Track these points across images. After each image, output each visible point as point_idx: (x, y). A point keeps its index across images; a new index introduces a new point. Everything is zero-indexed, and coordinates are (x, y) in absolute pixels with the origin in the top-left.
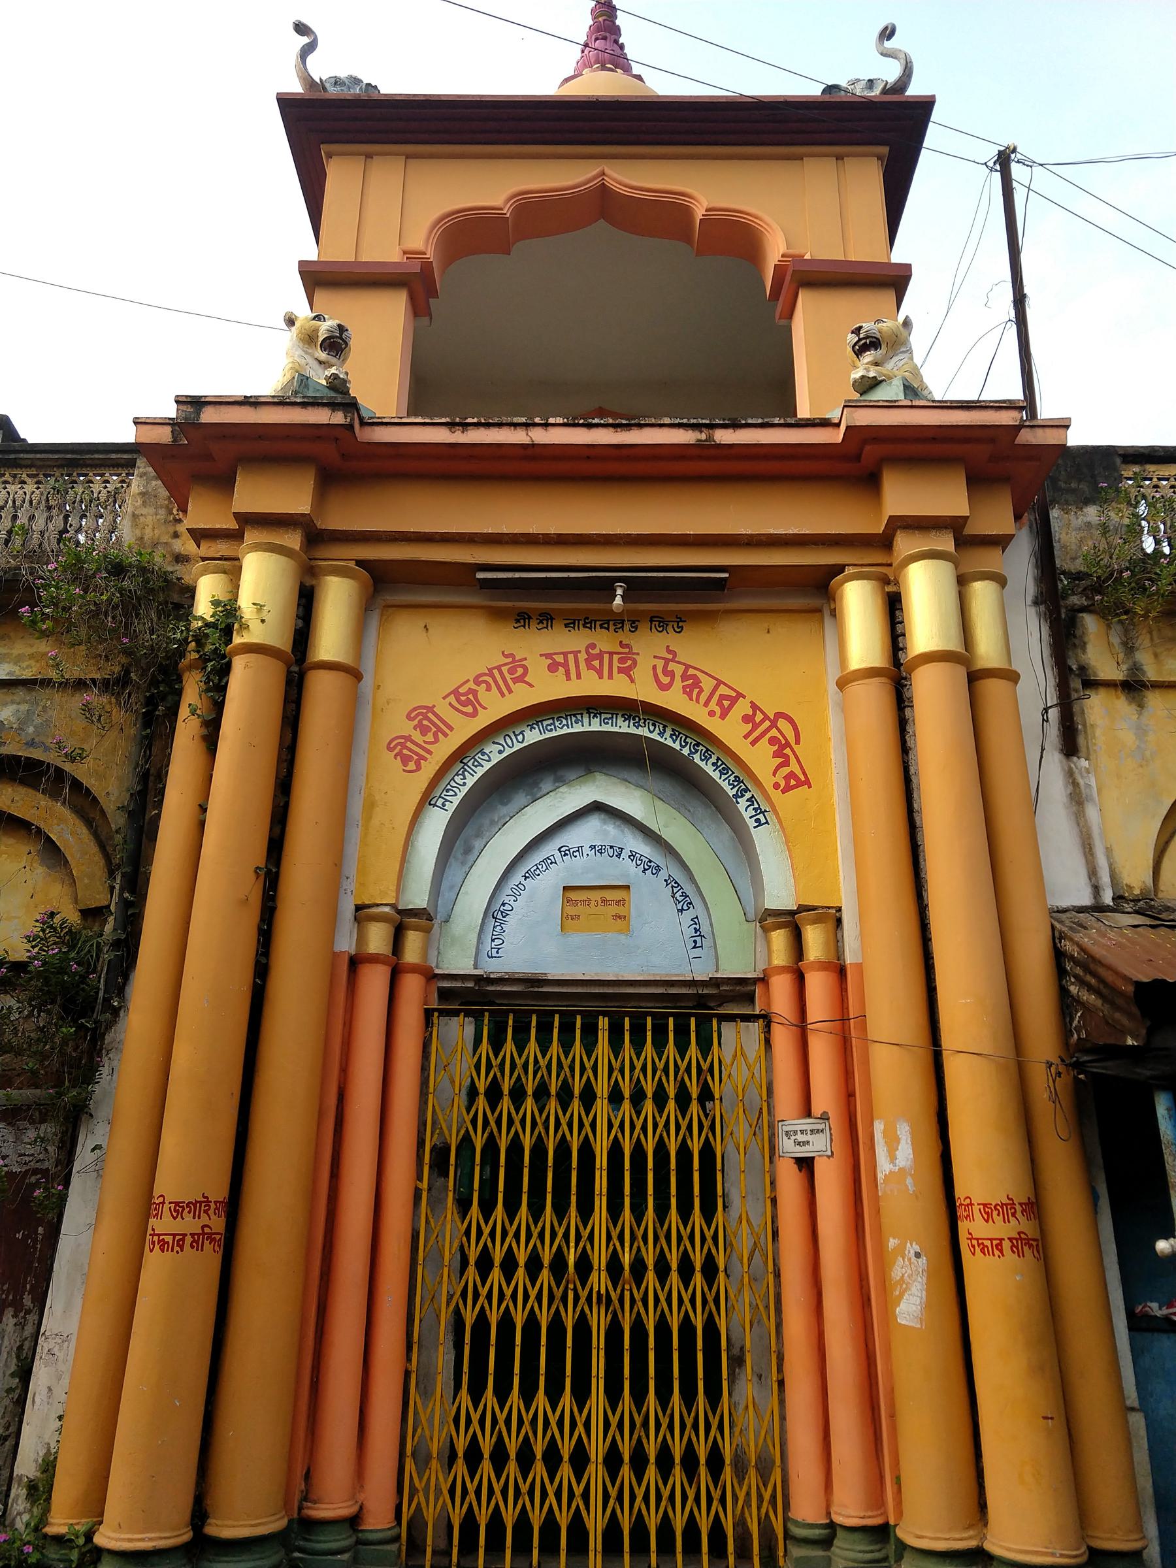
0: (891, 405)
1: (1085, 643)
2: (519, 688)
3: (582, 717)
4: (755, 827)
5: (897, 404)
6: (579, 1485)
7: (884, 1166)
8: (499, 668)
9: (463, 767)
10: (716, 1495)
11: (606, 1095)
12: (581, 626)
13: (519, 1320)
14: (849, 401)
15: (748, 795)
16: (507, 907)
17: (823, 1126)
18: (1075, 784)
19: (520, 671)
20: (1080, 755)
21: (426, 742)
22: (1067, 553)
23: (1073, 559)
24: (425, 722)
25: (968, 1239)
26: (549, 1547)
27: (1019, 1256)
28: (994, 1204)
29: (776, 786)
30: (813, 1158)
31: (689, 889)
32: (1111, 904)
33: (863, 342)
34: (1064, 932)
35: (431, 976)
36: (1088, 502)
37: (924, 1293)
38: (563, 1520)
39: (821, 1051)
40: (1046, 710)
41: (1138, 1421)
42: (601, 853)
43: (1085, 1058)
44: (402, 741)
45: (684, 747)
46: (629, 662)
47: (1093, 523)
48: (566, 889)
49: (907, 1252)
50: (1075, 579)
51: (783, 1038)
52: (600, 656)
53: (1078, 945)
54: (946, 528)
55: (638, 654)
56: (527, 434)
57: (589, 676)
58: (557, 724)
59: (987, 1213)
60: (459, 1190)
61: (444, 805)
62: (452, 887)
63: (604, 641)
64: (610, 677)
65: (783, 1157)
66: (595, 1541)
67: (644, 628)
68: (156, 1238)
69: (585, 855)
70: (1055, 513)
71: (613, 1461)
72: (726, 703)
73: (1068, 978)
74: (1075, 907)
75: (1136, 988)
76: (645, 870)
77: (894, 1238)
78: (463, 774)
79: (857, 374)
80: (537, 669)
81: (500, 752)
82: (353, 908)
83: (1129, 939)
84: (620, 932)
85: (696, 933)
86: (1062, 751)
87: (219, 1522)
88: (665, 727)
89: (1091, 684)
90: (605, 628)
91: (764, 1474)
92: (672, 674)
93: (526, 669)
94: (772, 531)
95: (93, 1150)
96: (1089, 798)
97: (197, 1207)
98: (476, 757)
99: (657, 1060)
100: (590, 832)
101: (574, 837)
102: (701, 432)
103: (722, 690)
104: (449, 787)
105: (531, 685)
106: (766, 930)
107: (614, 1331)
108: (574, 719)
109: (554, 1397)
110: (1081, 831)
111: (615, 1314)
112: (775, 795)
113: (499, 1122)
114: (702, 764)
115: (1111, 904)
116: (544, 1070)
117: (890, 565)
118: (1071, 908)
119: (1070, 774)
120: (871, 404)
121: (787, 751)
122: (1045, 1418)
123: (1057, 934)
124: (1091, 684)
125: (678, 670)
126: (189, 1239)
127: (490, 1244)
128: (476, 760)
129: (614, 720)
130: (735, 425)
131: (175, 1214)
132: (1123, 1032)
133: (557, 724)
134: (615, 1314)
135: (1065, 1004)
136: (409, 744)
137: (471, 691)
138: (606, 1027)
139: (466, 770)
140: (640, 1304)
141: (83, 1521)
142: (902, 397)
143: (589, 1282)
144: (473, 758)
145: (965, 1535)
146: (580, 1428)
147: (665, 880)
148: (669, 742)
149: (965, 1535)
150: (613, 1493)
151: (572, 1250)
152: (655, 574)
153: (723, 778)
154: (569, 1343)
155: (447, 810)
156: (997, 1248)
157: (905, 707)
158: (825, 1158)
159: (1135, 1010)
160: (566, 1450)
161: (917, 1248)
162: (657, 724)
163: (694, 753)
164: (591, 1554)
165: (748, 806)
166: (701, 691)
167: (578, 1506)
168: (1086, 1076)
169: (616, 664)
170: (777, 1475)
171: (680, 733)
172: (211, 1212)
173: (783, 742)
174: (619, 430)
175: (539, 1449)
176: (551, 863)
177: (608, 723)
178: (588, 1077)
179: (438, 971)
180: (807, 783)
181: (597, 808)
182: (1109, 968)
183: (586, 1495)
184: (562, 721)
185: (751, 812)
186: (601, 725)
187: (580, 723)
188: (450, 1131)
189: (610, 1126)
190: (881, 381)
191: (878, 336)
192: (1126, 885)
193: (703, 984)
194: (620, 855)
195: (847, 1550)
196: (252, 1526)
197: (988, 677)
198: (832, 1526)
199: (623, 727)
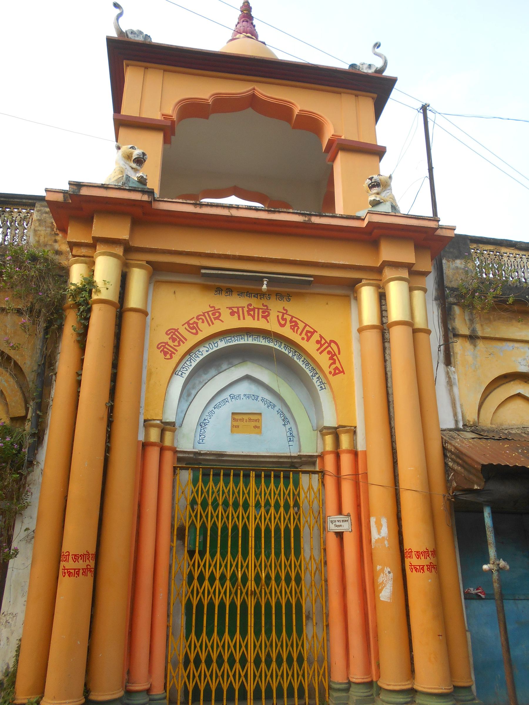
0: (387, 214)
1: (454, 319)
2: (217, 322)
3: (244, 337)
4: (320, 390)
5: (389, 214)
6: (243, 671)
7: (375, 535)
8: (208, 312)
9: (190, 358)
10: (301, 673)
11: (254, 505)
12: (245, 295)
13: (217, 603)
14: (370, 211)
15: (317, 376)
16: (206, 421)
17: (347, 519)
18: (449, 378)
19: (217, 314)
20: (452, 365)
21: (174, 346)
22: (449, 279)
23: (451, 282)
24: (174, 336)
25: (409, 566)
26: (231, 698)
27: (430, 572)
28: (421, 551)
29: (330, 373)
30: (343, 532)
31: (288, 415)
32: (462, 428)
33: (373, 183)
34: (447, 441)
35: (175, 451)
36: (457, 258)
37: (392, 588)
38: (237, 687)
39: (347, 488)
40: (440, 346)
41: (468, 635)
42: (249, 398)
43: (458, 493)
44: (164, 344)
45: (290, 352)
46: (267, 313)
47: (459, 267)
48: (233, 414)
49: (385, 571)
50: (451, 290)
51: (330, 482)
52: (253, 310)
53: (454, 446)
54: (405, 267)
55: (270, 310)
56: (229, 211)
57: (249, 318)
58: (233, 339)
59: (418, 555)
60: (189, 546)
61: (182, 374)
62: (182, 411)
63: (255, 303)
64: (258, 319)
65: (330, 531)
66: (250, 695)
67: (273, 298)
68: (66, 571)
69: (241, 399)
70: (444, 261)
71: (257, 661)
72: (309, 334)
73: (447, 459)
74: (448, 429)
75: (482, 467)
76: (268, 406)
77: (380, 565)
78: (190, 361)
79: (372, 198)
80: (225, 314)
81: (207, 351)
82: (143, 421)
83: (473, 444)
84: (257, 433)
85: (290, 435)
86: (445, 363)
87: (96, 694)
88: (281, 343)
89: (456, 335)
90: (256, 297)
91: (321, 662)
92: (285, 320)
93: (220, 314)
94: (333, 262)
95: (25, 530)
96: (455, 384)
97: (84, 557)
98: (196, 353)
99: (276, 490)
100: (244, 388)
101: (238, 390)
102: (306, 217)
103: (307, 328)
104: (184, 366)
105: (222, 321)
106: (323, 435)
107: (258, 606)
108: (240, 337)
109: (232, 634)
110: (451, 397)
111: (258, 599)
112: (330, 377)
113: (207, 516)
114: (298, 361)
115: (462, 428)
116: (227, 494)
117: (381, 280)
118: (447, 429)
119: (448, 373)
120: (379, 213)
121: (335, 357)
122: (439, 635)
123: (444, 441)
124: (456, 335)
125: (289, 318)
126: (81, 571)
127: (203, 570)
128: (196, 354)
129: (259, 339)
130: (320, 216)
131: (75, 560)
132: (473, 483)
133: (233, 339)
134: (258, 599)
135: (447, 469)
136: (167, 346)
137: (195, 322)
138: (254, 476)
139: (191, 359)
140: (269, 595)
141: (32, 697)
142: (390, 211)
143: (247, 586)
144: (195, 353)
145: (407, 683)
146: (243, 648)
147: (277, 411)
148: (283, 350)
149: (407, 683)
150: (258, 675)
151: (240, 572)
152: (281, 276)
153: (306, 368)
154: (239, 612)
155: (183, 377)
156: (422, 569)
157: (385, 342)
158: (349, 532)
159: (481, 476)
160: (237, 658)
161: (389, 570)
162: (278, 342)
163: (294, 356)
164: (249, 700)
165: (317, 381)
166: (298, 328)
167: (243, 681)
168: (455, 500)
169: (261, 314)
170: (325, 663)
171: (288, 346)
172: (90, 559)
173: (333, 353)
174: (270, 213)
175: (226, 657)
176: (226, 402)
177: (256, 340)
178: (246, 497)
179: (178, 449)
180: (343, 372)
181: (247, 378)
182: (469, 457)
183: (246, 676)
184: (235, 338)
185: (318, 383)
186: (253, 341)
187: (243, 339)
188: (185, 521)
189: (255, 518)
190: (382, 202)
191: (379, 182)
192: (468, 420)
193: (295, 457)
194: (257, 399)
195: (357, 692)
196: (111, 694)
197: (420, 332)
198: (349, 683)
199: (262, 342)
